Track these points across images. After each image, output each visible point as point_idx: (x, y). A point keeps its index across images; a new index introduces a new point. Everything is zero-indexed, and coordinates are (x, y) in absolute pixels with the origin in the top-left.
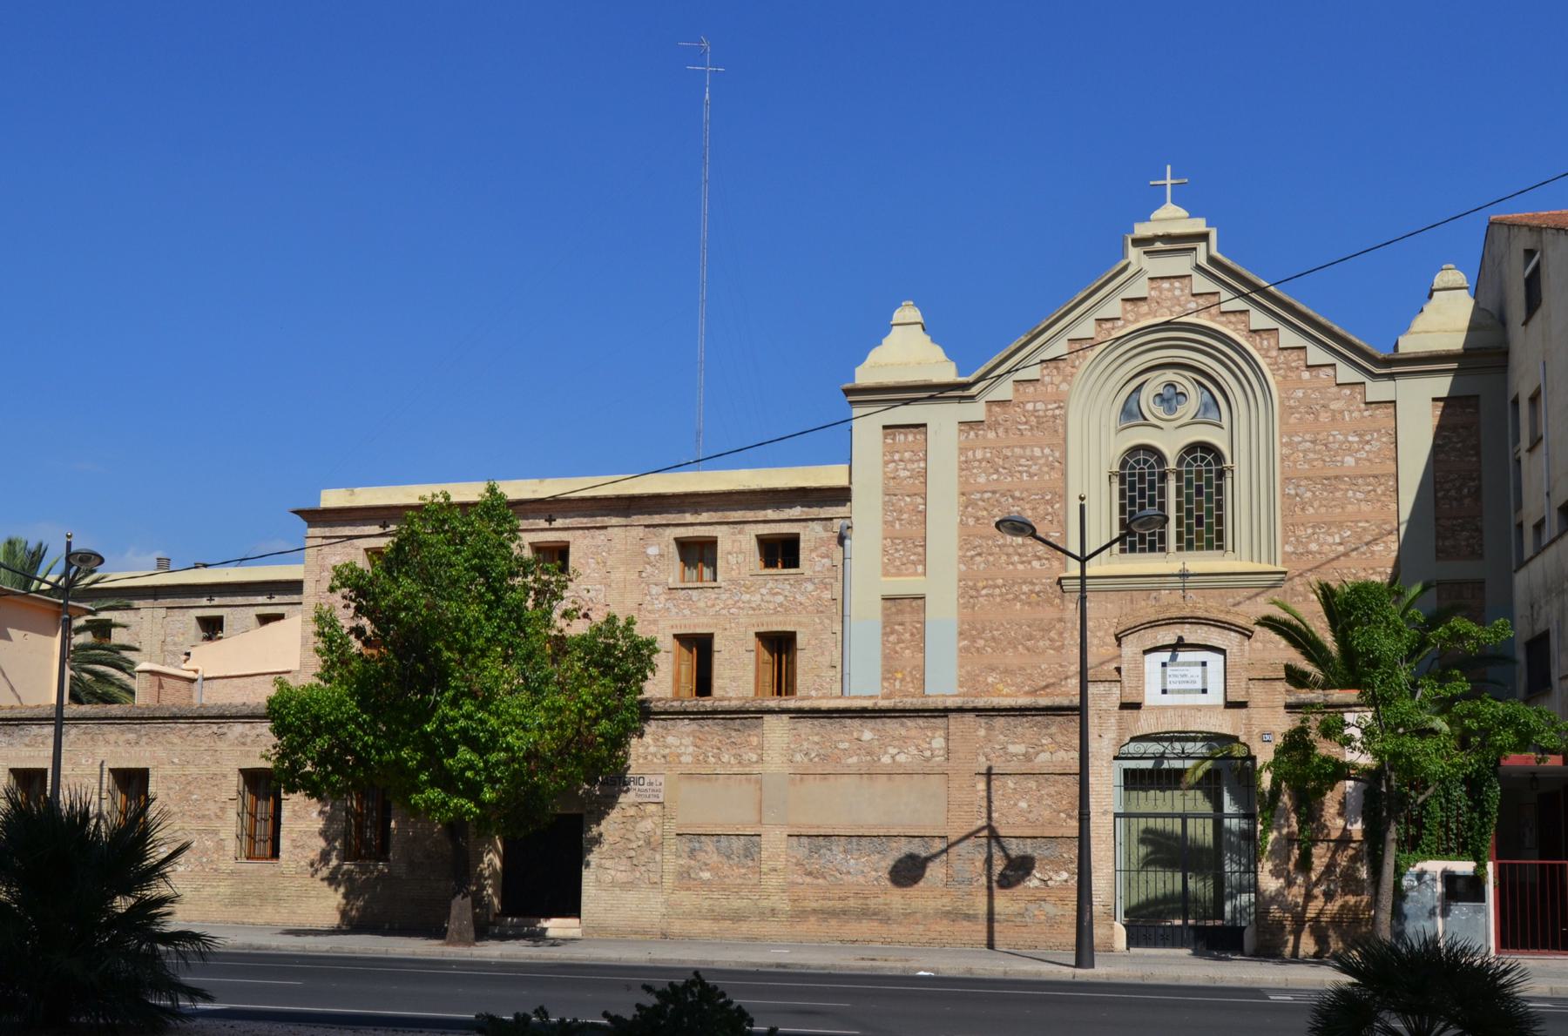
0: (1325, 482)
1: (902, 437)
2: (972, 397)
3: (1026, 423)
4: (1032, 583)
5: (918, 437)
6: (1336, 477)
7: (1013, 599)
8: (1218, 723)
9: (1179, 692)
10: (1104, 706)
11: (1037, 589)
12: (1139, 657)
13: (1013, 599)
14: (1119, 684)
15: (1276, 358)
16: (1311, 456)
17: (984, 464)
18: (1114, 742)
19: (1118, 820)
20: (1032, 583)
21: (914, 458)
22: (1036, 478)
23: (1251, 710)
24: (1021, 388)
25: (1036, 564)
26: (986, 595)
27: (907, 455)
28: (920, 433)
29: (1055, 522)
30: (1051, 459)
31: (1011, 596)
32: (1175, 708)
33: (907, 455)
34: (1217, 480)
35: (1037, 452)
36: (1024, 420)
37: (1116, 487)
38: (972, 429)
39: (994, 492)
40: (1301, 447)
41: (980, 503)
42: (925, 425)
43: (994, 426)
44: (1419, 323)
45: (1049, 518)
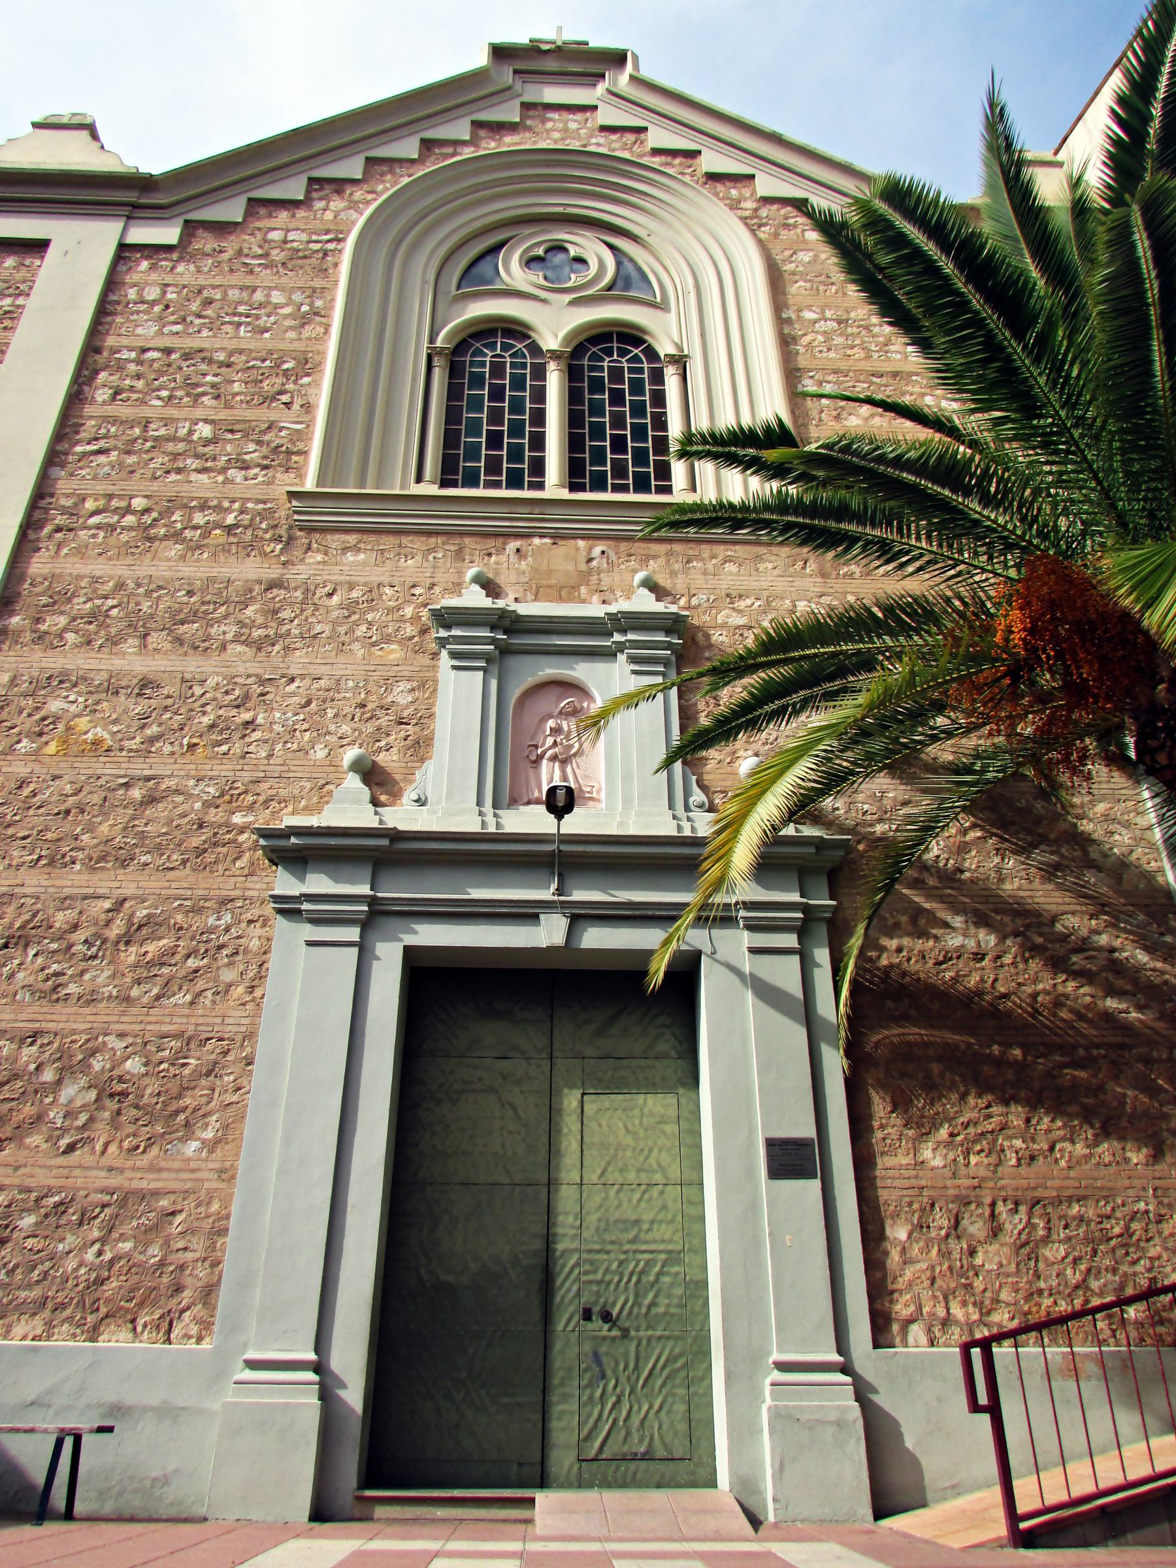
0: (874, 379)
3: (260, 256)
4: (219, 508)
6: (895, 375)
7: (166, 537)
11: (230, 519)
13: (166, 537)
15: (756, 210)
16: (838, 340)
17: (157, 309)
20: (219, 508)
22: (267, 335)
25: (236, 474)
26: (98, 527)
29: (296, 407)
30: (305, 308)
31: (162, 531)
34: (651, 383)
35: (277, 297)
36: (260, 252)
37: (439, 377)
38: (147, 258)
39: (168, 351)
40: (821, 326)
41: (132, 367)
43: (192, 258)
45: (285, 398)
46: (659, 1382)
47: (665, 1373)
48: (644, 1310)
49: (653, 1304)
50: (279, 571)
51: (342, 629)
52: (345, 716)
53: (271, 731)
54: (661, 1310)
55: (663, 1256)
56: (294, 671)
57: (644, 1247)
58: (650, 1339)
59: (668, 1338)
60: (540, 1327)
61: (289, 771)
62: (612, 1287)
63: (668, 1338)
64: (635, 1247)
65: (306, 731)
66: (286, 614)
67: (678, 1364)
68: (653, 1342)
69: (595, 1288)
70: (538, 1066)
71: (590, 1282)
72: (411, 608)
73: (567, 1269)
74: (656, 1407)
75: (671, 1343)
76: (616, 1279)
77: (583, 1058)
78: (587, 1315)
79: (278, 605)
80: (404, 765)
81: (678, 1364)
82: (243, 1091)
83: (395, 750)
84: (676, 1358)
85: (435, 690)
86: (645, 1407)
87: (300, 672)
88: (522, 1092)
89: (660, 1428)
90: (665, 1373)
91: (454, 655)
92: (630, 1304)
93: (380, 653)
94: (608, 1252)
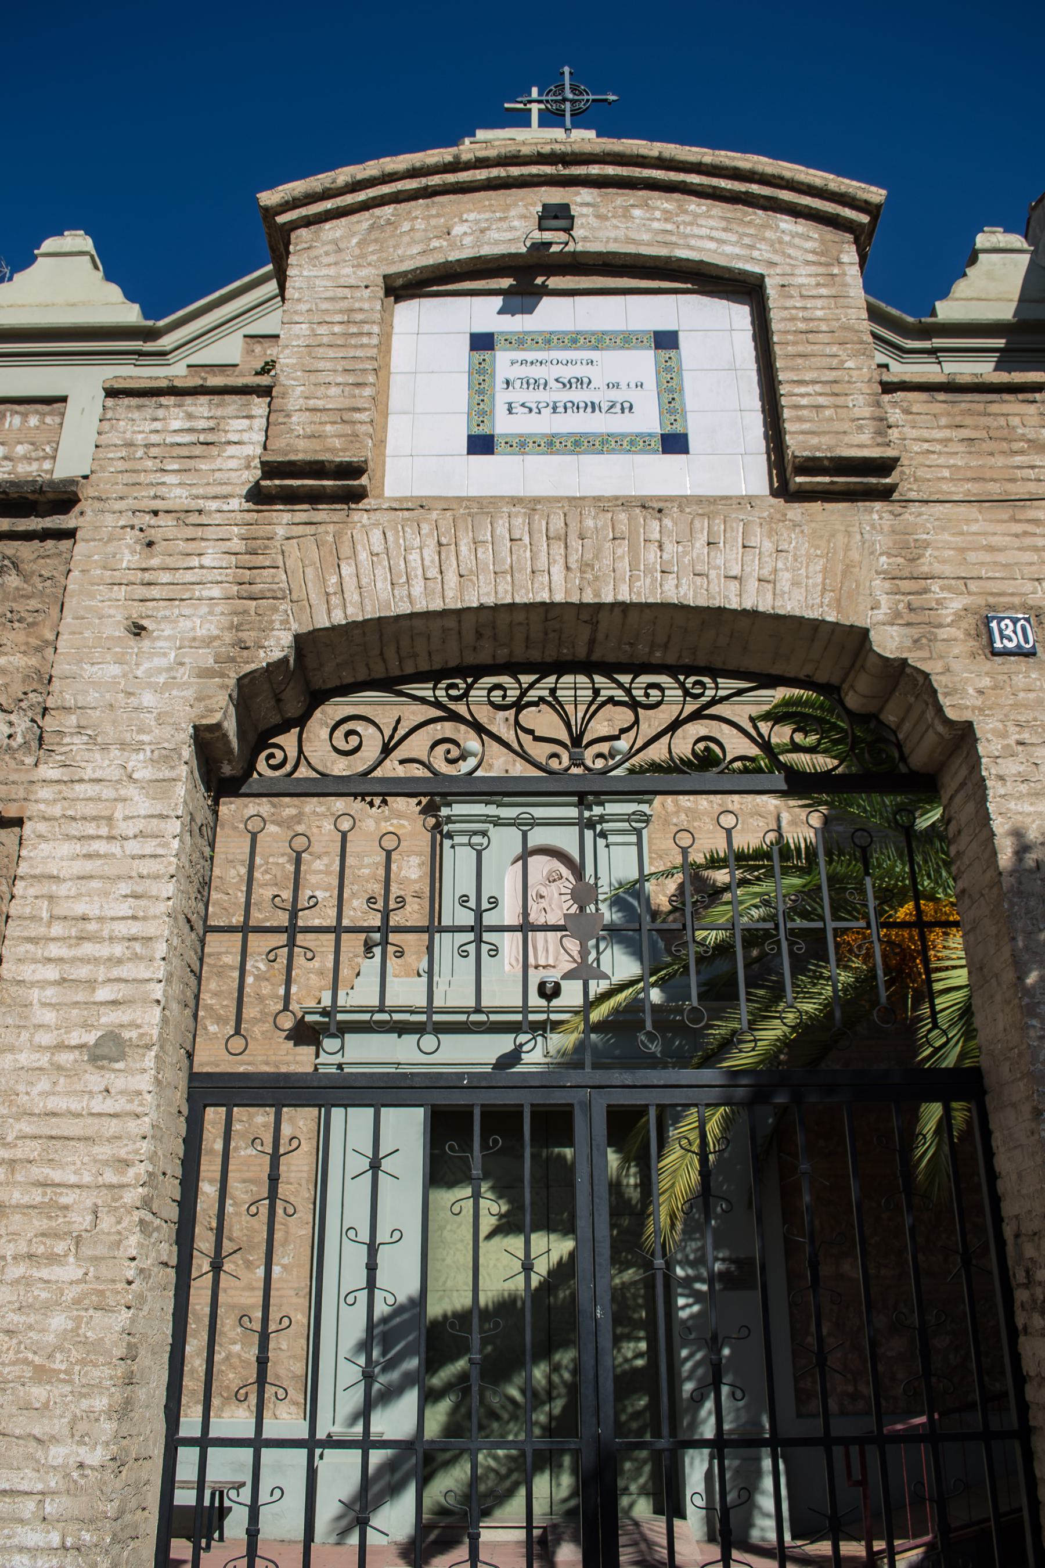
1: (17, 420)
2: (163, 354)
5: (48, 420)
8: (753, 569)
9: (551, 444)
10: (177, 495)
12: (371, 301)
14: (259, 406)
18: (206, 658)
19: (214, 1116)
21: (33, 455)
23: (910, 515)
24: (258, 349)
27: (20, 450)
28: (51, 414)
32: (532, 505)
33: (20, 450)
42: (64, 399)
44: (961, 288)
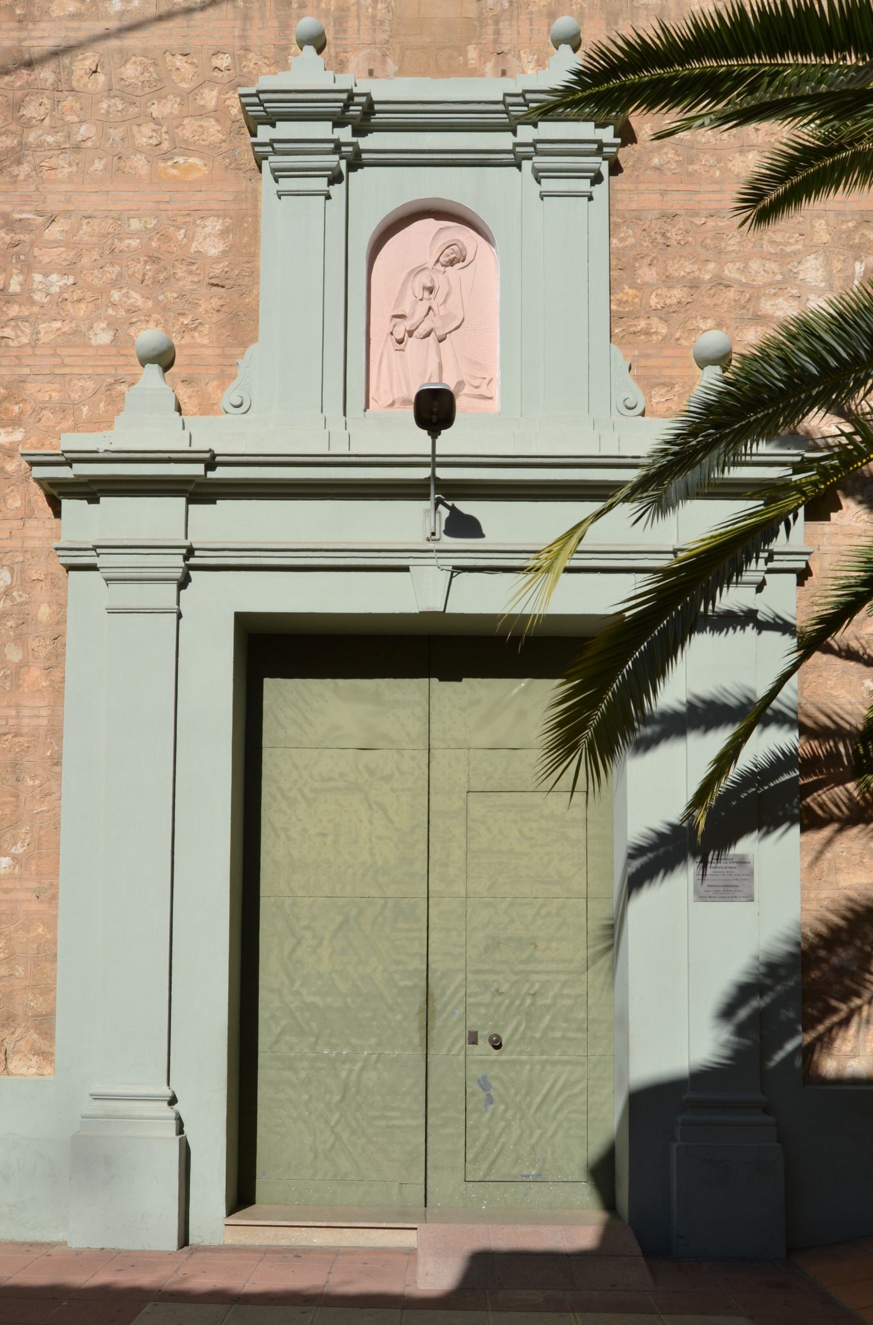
46: (555, 1106)
47: (560, 1100)
48: (538, 1035)
49: (550, 1028)
50: (14, 34)
51: (116, 133)
52: (132, 276)
53: (33, 303)
54: (558, 1034)
55: (563, 977)
56: (53, 204)
57: (541, 967)
58: (544, 1064)
59: (567, 1062)
60: (421, 1051)
61: (63, 365)
62: (503, 1009)
63: (567, 1062)
64: (530, 967)
65: (79, 301)
66: (31, 111)
67: (577, 1090)
68: (548, 1068)
69: (483, 1011)
70: (413, 758)
71: (480, 1004)
72: (215, 93)
73: (449, 992)
74: (549, 1133)
75: (568, 1068)
76: (507, 1002)
77: (469, 749)
78: (473, 1039)
79: (19, 94)
80: (218, 351)
81: (577, 1090)
82: (54, 797)
83: (206, 329)
84: (577, 1082)
85: (256, 230)
86: (538, 1132)
87: (62, 207)
88: (393, 790)
89: (553, 1153)
90: (560, 1100)
91: (278, 174)
92: (522, 1028)
93: (174, 172)
94: (497, 973)
